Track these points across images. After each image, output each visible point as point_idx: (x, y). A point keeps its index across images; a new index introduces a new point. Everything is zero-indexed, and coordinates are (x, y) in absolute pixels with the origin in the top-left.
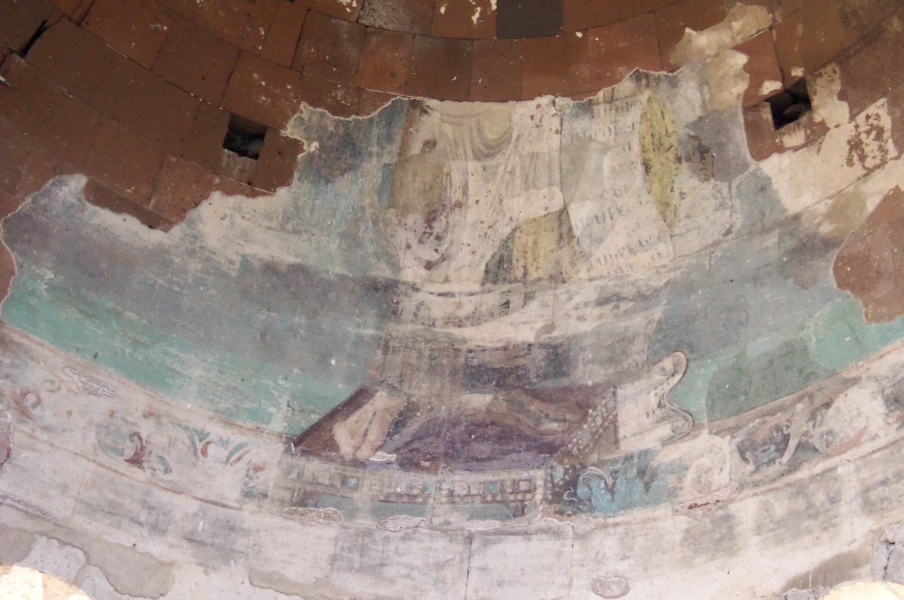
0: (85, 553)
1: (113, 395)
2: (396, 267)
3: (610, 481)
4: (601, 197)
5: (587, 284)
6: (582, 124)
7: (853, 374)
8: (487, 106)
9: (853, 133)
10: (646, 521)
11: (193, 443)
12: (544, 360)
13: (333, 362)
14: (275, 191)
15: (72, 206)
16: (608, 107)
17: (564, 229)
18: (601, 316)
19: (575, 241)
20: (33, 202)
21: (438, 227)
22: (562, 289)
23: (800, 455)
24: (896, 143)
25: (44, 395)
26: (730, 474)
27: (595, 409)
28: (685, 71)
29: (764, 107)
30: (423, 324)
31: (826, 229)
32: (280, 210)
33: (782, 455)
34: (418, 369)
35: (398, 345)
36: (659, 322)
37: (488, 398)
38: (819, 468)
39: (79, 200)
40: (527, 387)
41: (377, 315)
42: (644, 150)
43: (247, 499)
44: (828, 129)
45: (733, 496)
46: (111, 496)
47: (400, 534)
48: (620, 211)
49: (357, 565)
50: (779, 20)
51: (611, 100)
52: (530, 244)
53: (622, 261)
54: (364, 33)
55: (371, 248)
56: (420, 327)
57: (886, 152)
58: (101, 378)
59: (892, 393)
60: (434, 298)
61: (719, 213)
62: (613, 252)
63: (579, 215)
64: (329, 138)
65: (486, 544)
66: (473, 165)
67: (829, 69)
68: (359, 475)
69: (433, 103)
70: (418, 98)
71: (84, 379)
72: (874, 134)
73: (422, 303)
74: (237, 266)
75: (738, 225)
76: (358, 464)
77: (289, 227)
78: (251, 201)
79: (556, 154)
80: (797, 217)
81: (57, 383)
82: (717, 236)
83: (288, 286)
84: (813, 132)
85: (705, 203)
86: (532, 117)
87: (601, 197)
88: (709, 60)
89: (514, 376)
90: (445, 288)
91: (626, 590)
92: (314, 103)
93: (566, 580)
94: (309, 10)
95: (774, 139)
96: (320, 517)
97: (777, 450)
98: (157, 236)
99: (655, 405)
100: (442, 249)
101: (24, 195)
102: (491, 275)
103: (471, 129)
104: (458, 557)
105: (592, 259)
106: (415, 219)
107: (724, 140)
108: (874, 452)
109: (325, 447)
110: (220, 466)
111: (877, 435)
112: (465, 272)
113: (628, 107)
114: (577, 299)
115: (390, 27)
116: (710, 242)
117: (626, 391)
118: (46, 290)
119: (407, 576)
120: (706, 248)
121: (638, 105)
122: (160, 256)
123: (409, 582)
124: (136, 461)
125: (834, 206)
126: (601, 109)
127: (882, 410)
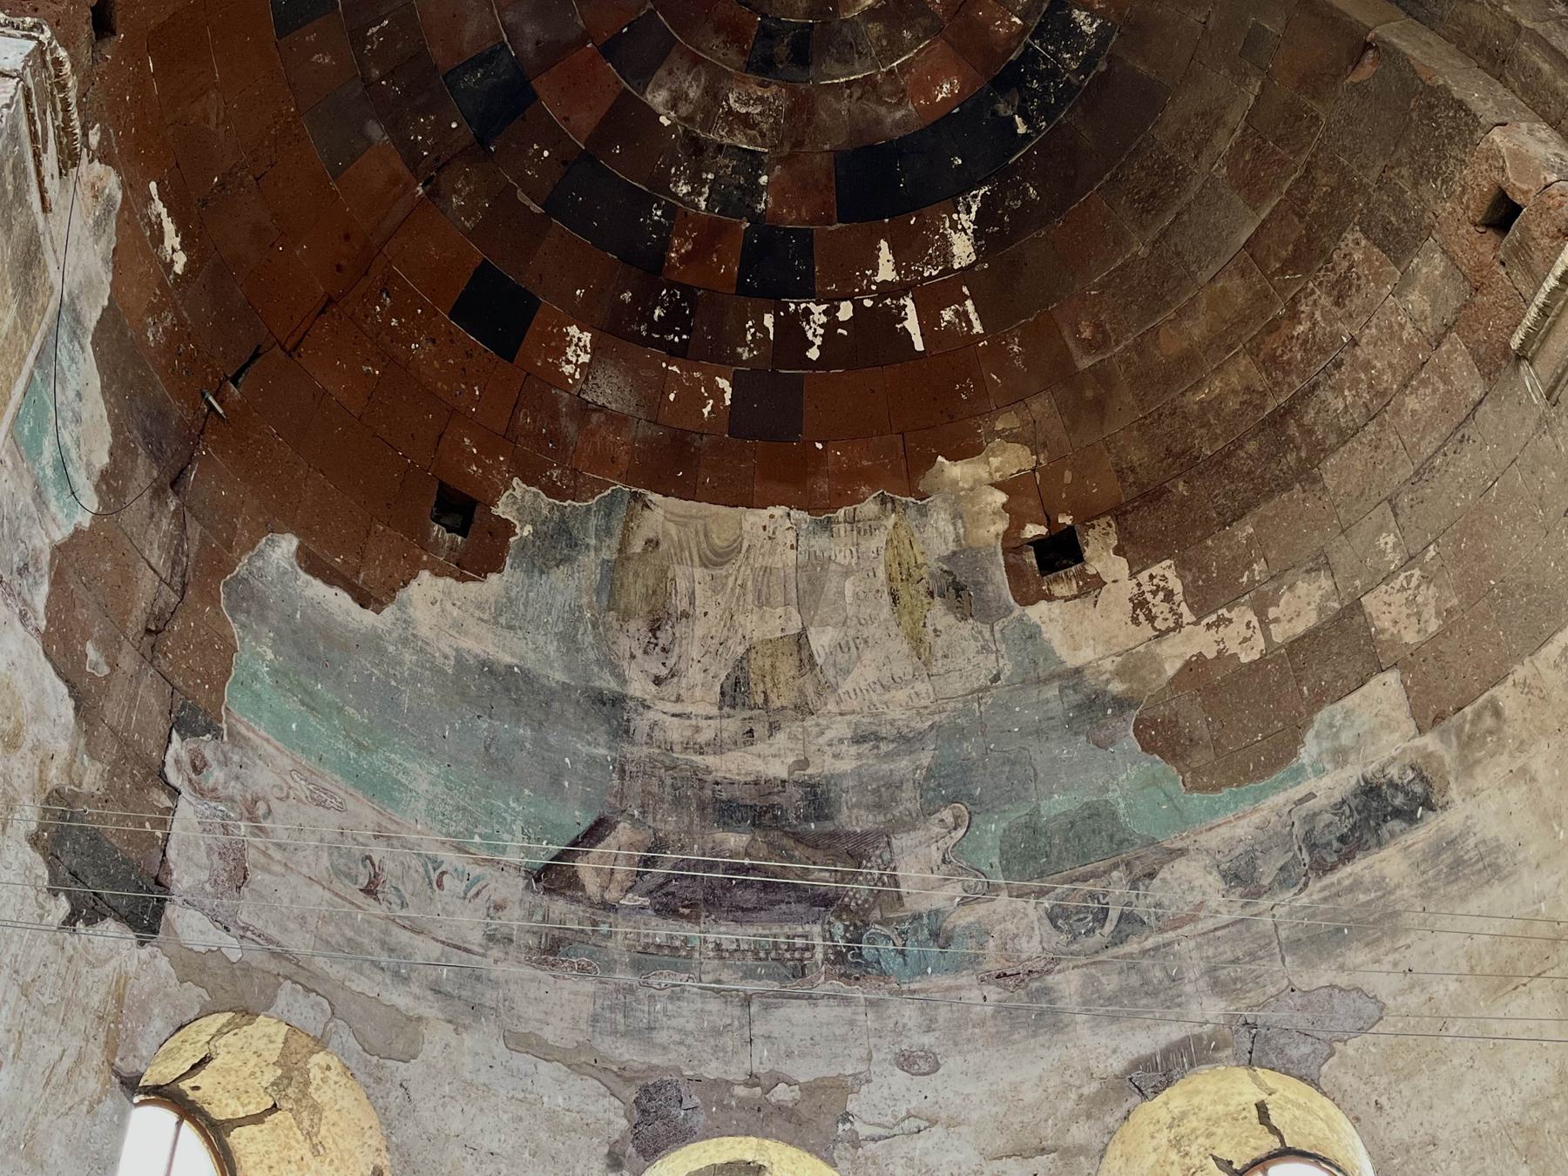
0: (330, 1004)
1: (341, 809)
2: (624, 681)
3: (899, 942)
4: (844, 623)
5: (839, 718)
6: (820, 542)
7: (1178, 845)
8: (714, 508)
9: (1136, 591)
10: (949, 989)
11: (427, 871)
12: (801, 799)
13: (566, 784)
14: (485, 577)
15: (285, 573)
16: (848, 527)
17: (805, 654)
18: (859, 756)
19: (818, 669)
20: (249, 563)
21: (664, 638)
22: (810, 722)
23: (1127, 928)
24: (1191, 607)
25: (275, 804)
26: (1041, 942)
27: (869, 860)
28: (935, 501)
29: (1027, 551)
30: (659, 747)
31: (1117, 687)
32: (492, 600)
33: (1103, 926)
34: (662, 800)
35: (634, 769)
36: (929, 769)
37: (745, 838)
38: (1149, 943)
39: (292, 567)
40: (787, 829)
41: (608, 733)
42: (890, 579)
43: (491, 944)
44: (1105, 583)
45: (1049, 967)
46: (350, 934)
47: (668, 992)
48: (866, 642)
49: (621, 1028)
50: (1044, 463)
51: (852, 521)
52: (767, 667)
53: (875, 698)
54: (584, 410)
55: (592, 655)
56: (657, 751)
57: (1181, 616)
58: (328, 786)
59: (1229, 868)
60: (668, 719)
61: (981, 657)
62: (863, 685)
63: (821, 641)
64: (544, 523)
65: (767, 1007)
66: (699, 572)
67: (1103, 521)
68: (611, 920)
69: (655, 497)
70: (640, 490)
71: (311, 787)
72: (1161, 595)
73: (656, 723)
74: (452, 663)
75: (1007, 672)
76: (609, 907)
77: (503, 620)
78: (461, 585)
79: (791, 572)
80: (1078, 671)
81: (285, 789)
82: (984, 681)
83: (508, 690)
84: (1086, 583)
85: (964, 644)
86: (764, 528)
87: (844, 623)
88: (962, 493)
89: (769, 815)
90: (678, 708)
91: (936, 1067)
92: (528, 481)
93: (864, 1053)
94: (528, 374)
95: (1040, 586)
96: (573, 968)
97: (1094, 920)
98: (367, 617)
99: (939, 861)
100: (671, 662)
101: (242, 553)
102: (727, 698)
103: (697, 532)
104: (736, 1023)
105: (840, 691)
106: (638, 626)
107: (982, 580)
108: (1216, 929)
109: (569, 887)
110: (459, 902)
111: (1217, 912)
112: (698, 693)
113: (871, 531)
114: (829, 735)
115: (614, 406)
116: (976, 686)
117: (901, 841)
118: (268, 673)
119: (681, 1043)
120: (972, 693)
121: (882, 529)
122: (372, 643)
123: (683, 1049)
124: (370, 891)
125: (1124, 665)
126: (842, 528)
127: (1222, 886)
